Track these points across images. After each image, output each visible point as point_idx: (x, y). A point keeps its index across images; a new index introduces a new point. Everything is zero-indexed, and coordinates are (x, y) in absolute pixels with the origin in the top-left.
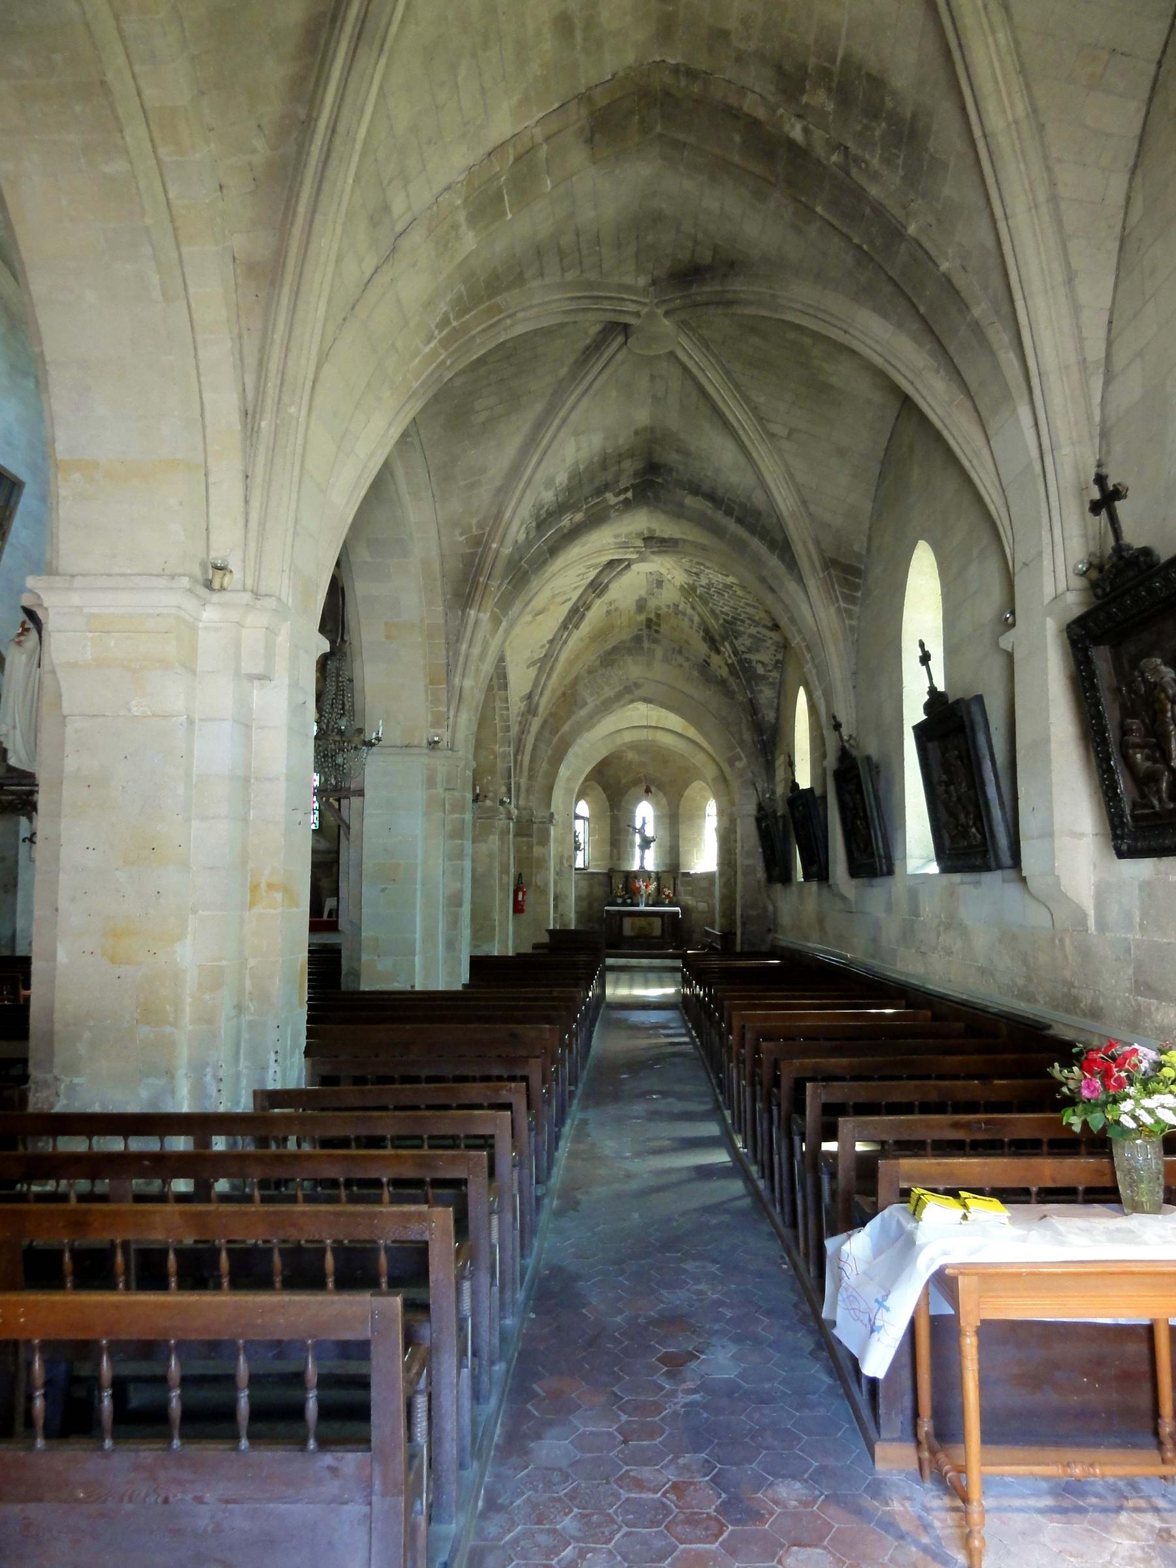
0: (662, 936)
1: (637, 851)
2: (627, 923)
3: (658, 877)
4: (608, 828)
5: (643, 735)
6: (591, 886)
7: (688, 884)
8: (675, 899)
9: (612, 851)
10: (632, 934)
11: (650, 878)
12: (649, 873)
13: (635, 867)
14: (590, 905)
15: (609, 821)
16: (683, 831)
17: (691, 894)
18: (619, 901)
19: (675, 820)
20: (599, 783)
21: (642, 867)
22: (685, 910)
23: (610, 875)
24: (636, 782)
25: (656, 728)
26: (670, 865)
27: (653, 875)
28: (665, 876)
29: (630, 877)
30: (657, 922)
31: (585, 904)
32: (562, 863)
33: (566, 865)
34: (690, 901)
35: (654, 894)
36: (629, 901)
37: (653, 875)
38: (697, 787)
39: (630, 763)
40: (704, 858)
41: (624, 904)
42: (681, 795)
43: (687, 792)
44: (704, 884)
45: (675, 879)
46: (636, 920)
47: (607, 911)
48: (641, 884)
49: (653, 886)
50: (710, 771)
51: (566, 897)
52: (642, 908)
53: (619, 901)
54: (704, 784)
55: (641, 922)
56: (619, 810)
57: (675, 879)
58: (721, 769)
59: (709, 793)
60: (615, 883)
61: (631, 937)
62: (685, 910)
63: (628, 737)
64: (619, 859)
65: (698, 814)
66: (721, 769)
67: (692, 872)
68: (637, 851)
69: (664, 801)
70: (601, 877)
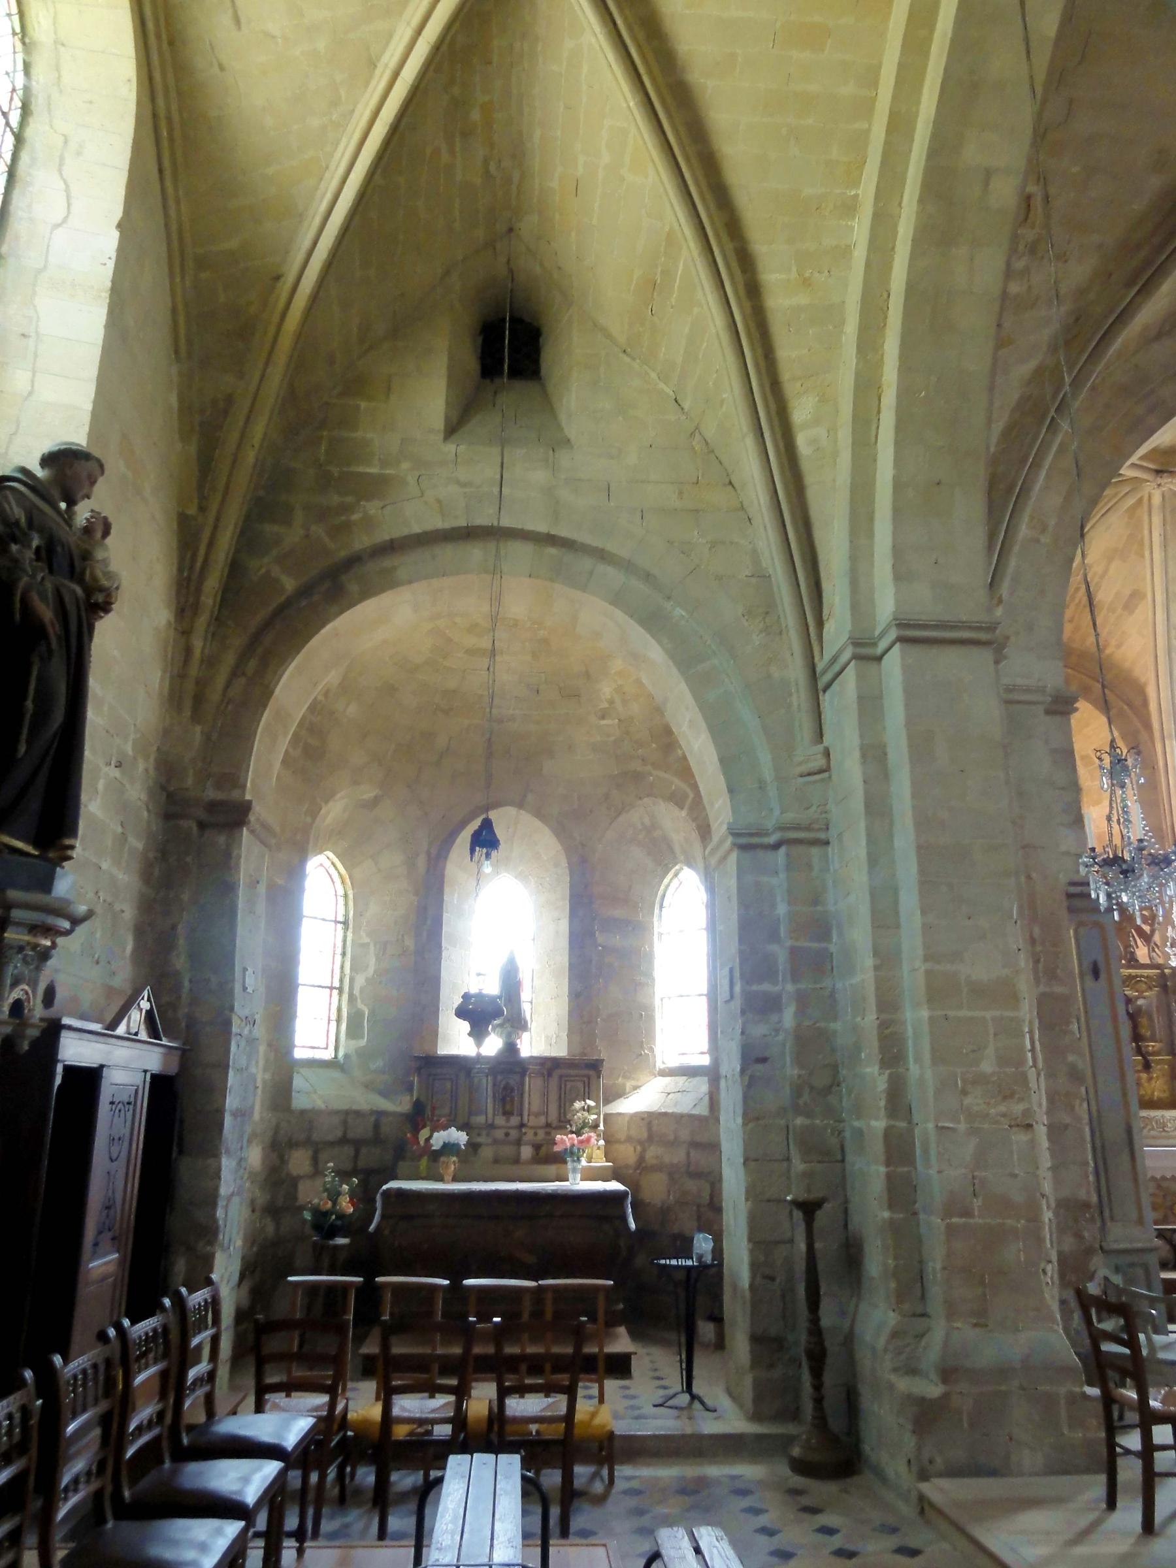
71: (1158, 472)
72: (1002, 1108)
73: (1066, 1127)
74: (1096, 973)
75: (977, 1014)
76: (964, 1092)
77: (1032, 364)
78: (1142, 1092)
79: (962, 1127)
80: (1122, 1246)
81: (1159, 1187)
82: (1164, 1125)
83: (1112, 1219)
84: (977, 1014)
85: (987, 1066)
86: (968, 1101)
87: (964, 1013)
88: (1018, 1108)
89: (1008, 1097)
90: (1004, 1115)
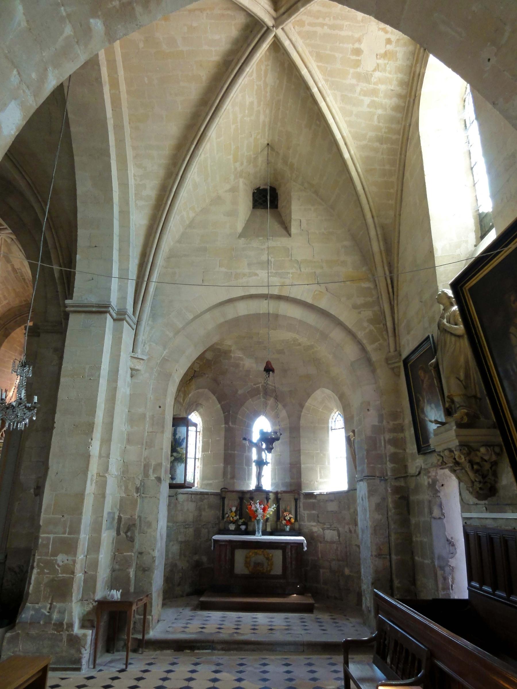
0: (284, 575)
1: (254, 468)
2: (240, 555)
3: (278, 498)
4: (222, 442)
5: (263, 307)
6: (199, 509)
7: (313, 507)
8: (297, 526)
9: (225, 468)
10: (246, 572)
11: (268, 499)
12: (267, 493)
13: (252, 486)
14: (197, 533)
15: (223, 433)
16: (305, 446)
17: (316, 519)
18: (232, 527)
19: (295, 440)
20: (214, 393)
21: (259, 488)
22: (311, 538)
23: (222, 496)
24: (254, 393)
25: (279, 298)
26: (291, 485)
27: (272, 496)
28: (287, 496)
29: (245, 498)
30: (277, 555)
31: (191, 530)
32: (146, 475)
33: (152, 477)
34: (316, 528)
35: (272, 519)
36: (243, 527)
37: (272, 496)
38: (322, 395)
39: (248, 371)
40: (332, 473)
41: (238, 531)
42: (302, 406)
43: (309, 403)
44: (332, 507)
45: (296, 500)
46: (251, 553)
47: (216, 541)
48: (258, 507)
49: (271, 510)
50: (351, 351)
51: (149, 525)
52: (259, 537)
53: (232, 527)
54: (328, 392)
55: (259, 556)
56: (234, 422)
57: (296, 500)
58: (363, 349)
59: (334, 402)
60: (232, 504)
61: (244, 577)
62: (311, 538)
63: (243, 309)
64: (233, 477)
65: (321, 427)
66: (363, 349)
67: (316, 492)
68: (254, 468)
69: (284, 413)
70: (212, 499)
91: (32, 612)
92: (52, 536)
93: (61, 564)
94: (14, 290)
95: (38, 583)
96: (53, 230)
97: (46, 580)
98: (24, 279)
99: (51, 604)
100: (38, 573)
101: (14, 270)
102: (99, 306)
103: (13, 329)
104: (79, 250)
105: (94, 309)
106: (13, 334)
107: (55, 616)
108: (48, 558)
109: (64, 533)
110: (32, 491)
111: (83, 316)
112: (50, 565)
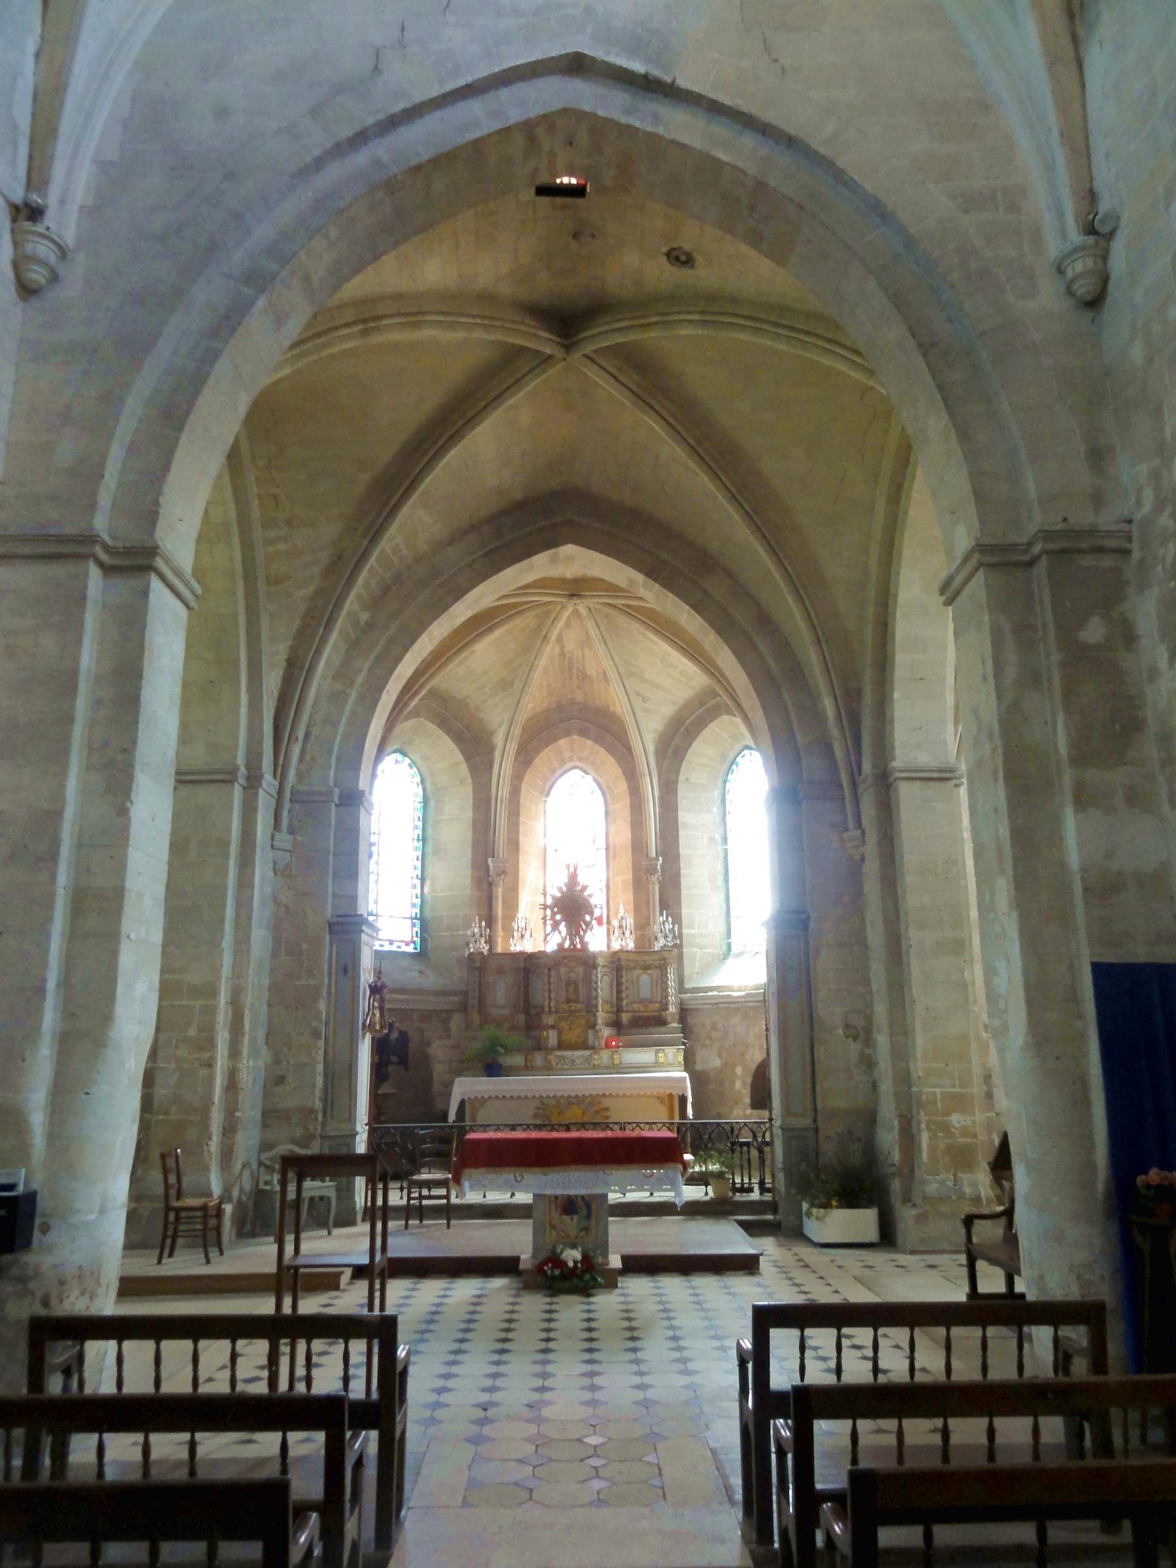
71: (572, 596)
72: (197, 1056)
73: (305, 1064)
74: (345, 971)
75: (191, 1003)
76: (177, 1047)
77: (311, 588)
78: (564, 1038)
79: (172, 1066)
80: (333, 1134)
81: (542, 1103)
82: (573, 1061)
83: (332, 1117)
84: (191, 1003)
85: (192, 1032)
86: (178, 1052)
87: (183, 1003)
88: (206, 1055)
89: (201, 1049)
90: (197, 1059)
91: (935, 1186)
92: (938, 1091)
93: (957, 1125)
94: (549, 686)
95: (933, 1150)
96: (823, 644)
97: (942, 1147)
98: (571, 668)
99: (955, 1175)
100: (931, 1138)
101: (562, 654)
102: (940, 770)
103: (538, 751)
104: (897, 685)
105: (935, 775)
106: (537, 761)
107: (968, 1190)
108: (940, 1118)
109: (954, 1086)
110: (840, 1031)
111: (918, 784)
112: (946, 1128)
